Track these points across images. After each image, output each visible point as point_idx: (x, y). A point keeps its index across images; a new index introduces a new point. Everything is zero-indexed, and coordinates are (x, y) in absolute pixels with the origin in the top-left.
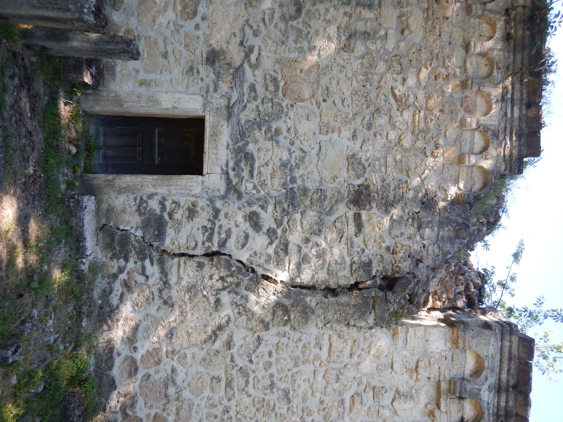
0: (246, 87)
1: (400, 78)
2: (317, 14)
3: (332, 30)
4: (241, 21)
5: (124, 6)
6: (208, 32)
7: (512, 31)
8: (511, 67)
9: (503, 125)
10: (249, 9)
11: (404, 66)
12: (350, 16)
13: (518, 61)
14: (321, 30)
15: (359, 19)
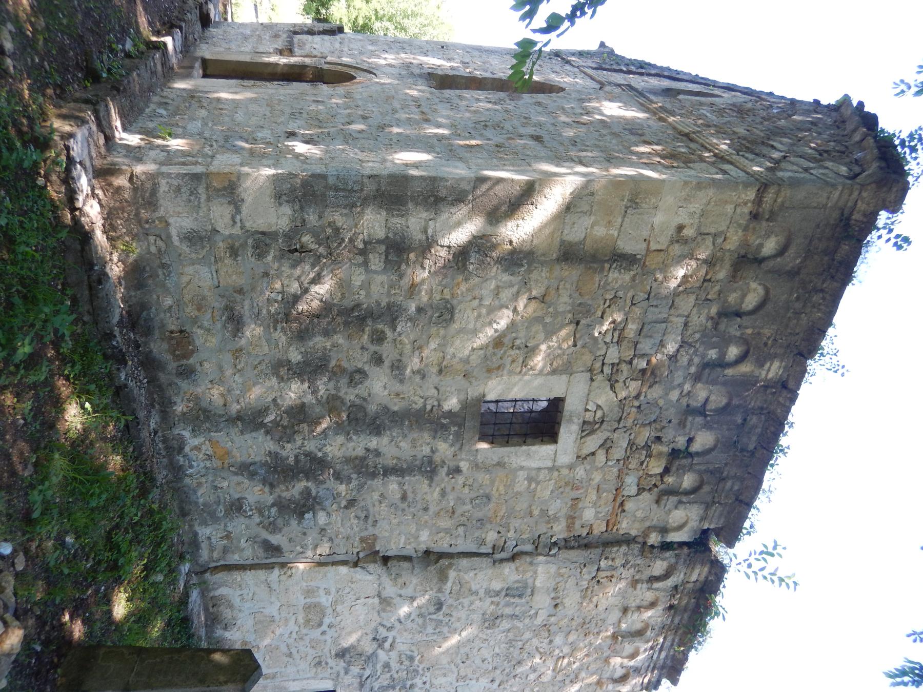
0: (379, 667)
1: (547, 641)
2: (460, 607)
3: (477, 617)
4: (373, 625)
5: (237, 626)
6: (336, 635)
7: (676, 602)
8: (666, 627)
9: (647, 664)
10: (383, 614)
11: (552, 631)
12: (498, 604)
13: (676, 621)
14: (464, 617)
15: (507, 605)
